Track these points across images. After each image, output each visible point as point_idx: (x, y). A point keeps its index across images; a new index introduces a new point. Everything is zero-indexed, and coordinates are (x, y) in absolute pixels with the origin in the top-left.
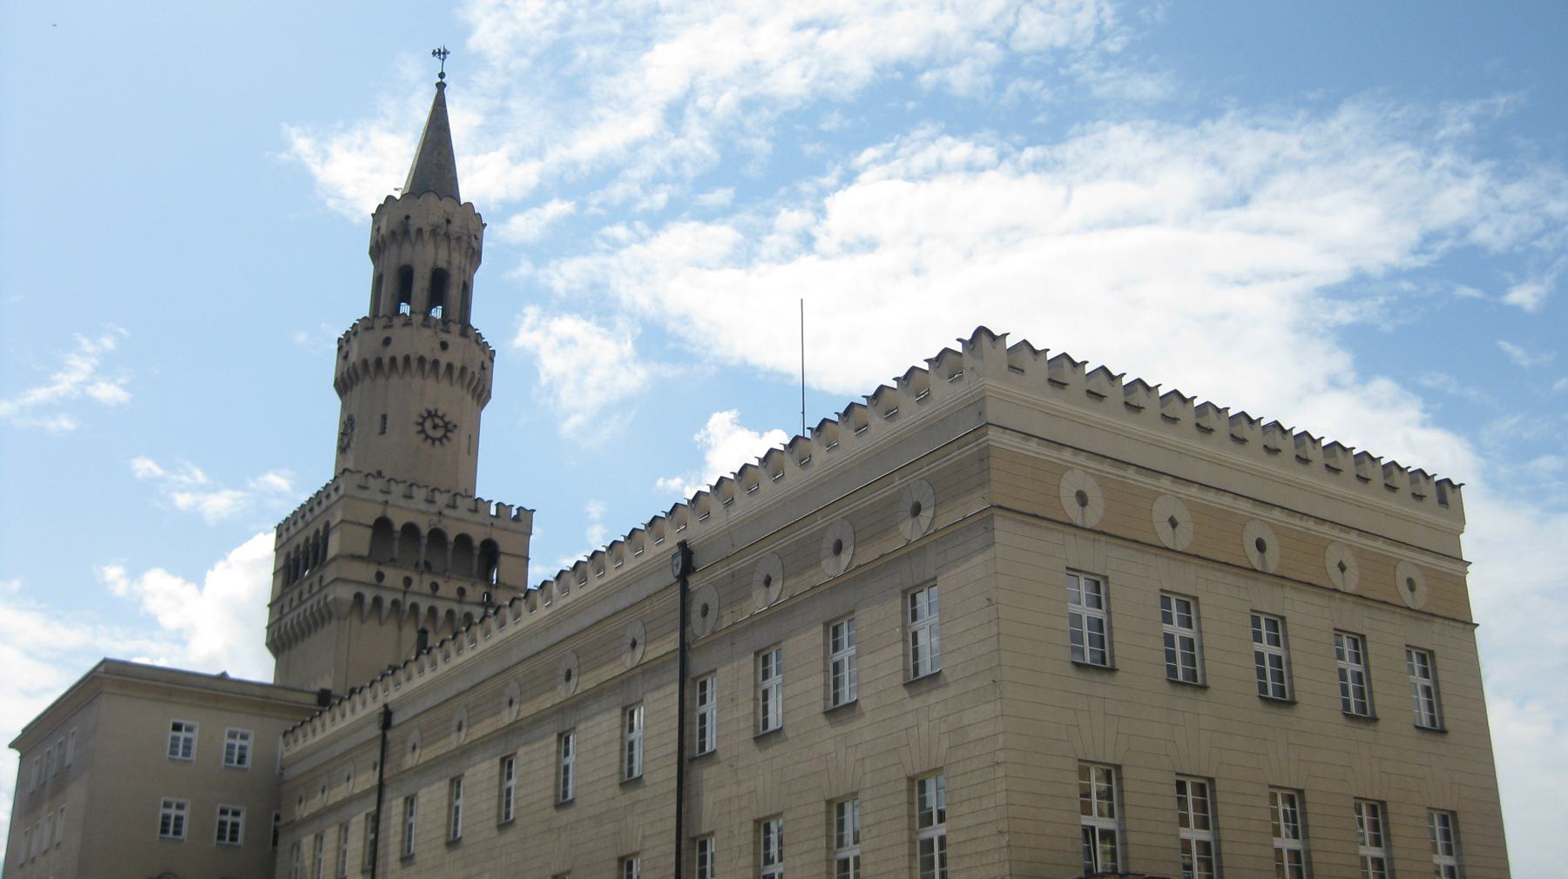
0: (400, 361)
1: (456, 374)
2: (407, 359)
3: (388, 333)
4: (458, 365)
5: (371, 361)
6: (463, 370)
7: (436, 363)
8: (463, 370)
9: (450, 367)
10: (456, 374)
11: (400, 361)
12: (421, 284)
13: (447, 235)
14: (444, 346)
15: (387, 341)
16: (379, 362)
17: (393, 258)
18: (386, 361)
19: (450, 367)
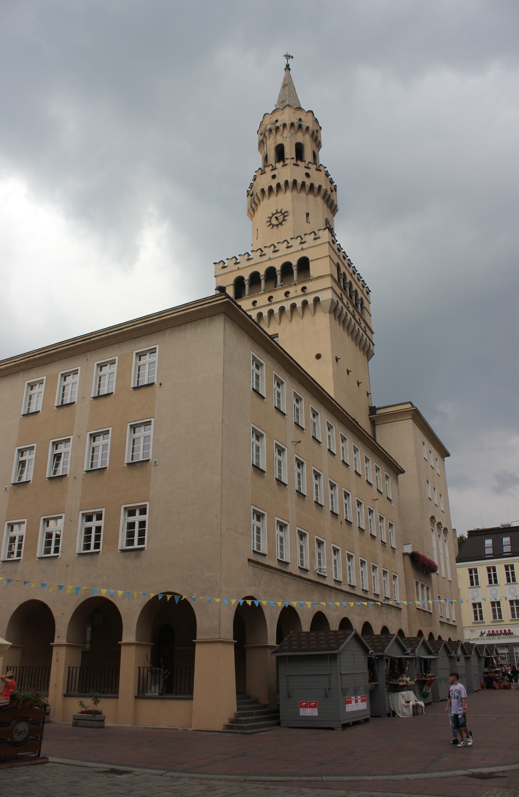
0: (282, 184)
1: (316, 190)
2: (286, 182)
3: (274, 172)
4: (316, 185)
5: (266, 189)
6: (320, 187)
7: (303, 184)
8: (320, 187)
9: (312, 185)
10: (316, 190)
11: (282, 184)
12: (290, 152)
13: (300, 126)
14: (307, 175)
15: (274, 177)
16: (270, 188)
17: (271, 144)
18: (274, 186)
19: (312, 185)
